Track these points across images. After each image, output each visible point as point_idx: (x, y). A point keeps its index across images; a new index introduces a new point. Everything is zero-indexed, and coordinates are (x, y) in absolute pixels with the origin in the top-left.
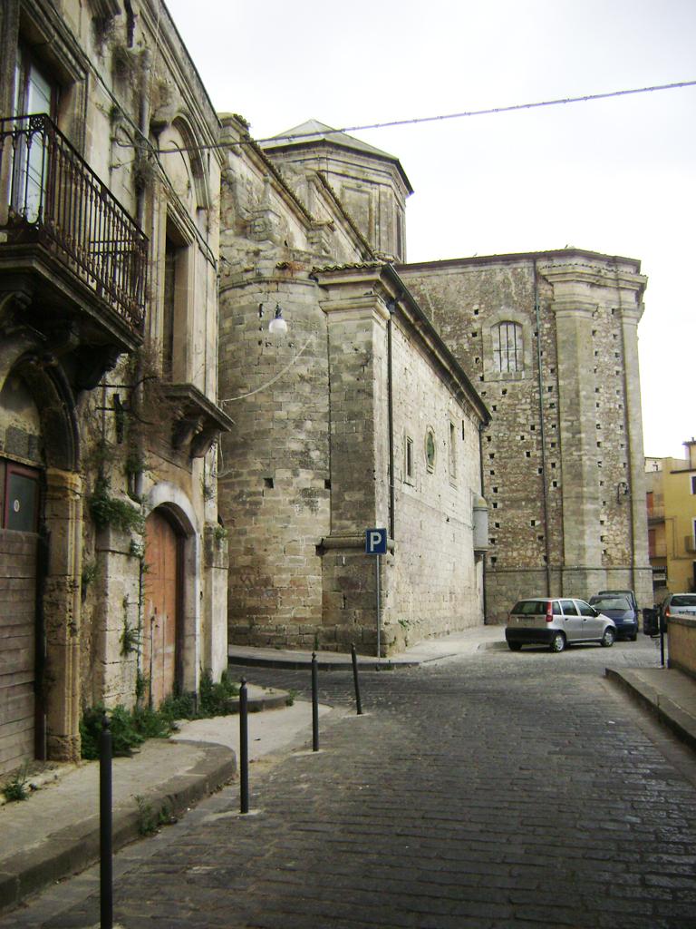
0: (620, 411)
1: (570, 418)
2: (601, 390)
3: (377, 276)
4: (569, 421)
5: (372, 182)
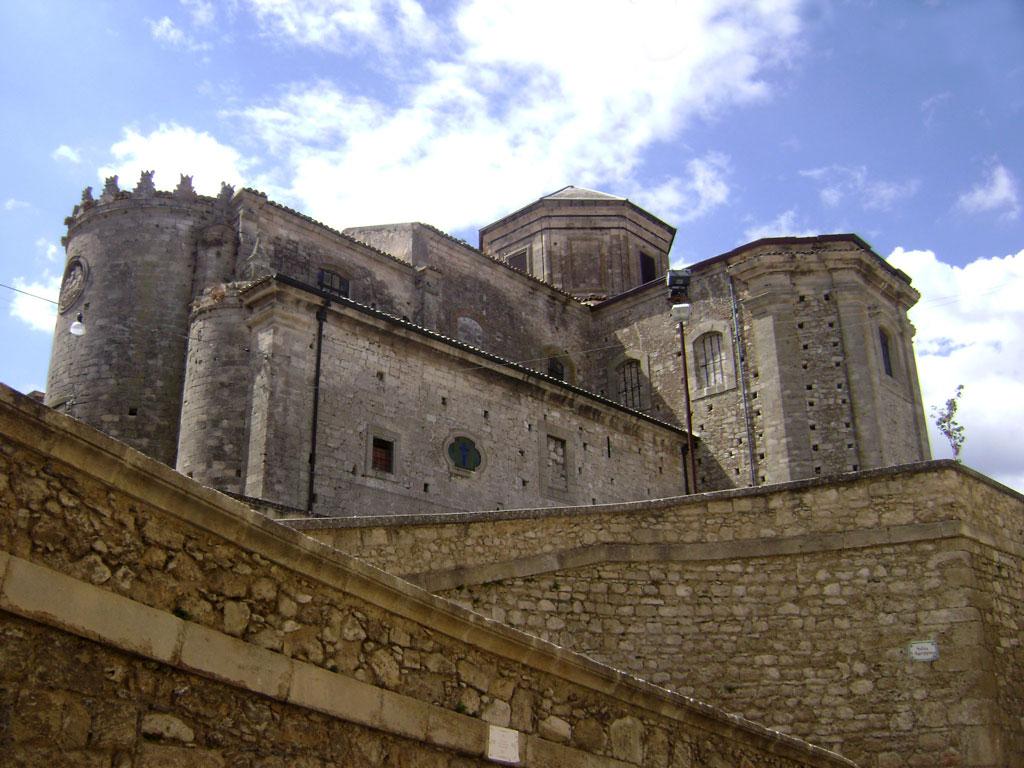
0: (844, 406)
1: (774, 423)
2: (814, 386)
3: (274, 287)
4: (773, 426)
5: (601, 229)
